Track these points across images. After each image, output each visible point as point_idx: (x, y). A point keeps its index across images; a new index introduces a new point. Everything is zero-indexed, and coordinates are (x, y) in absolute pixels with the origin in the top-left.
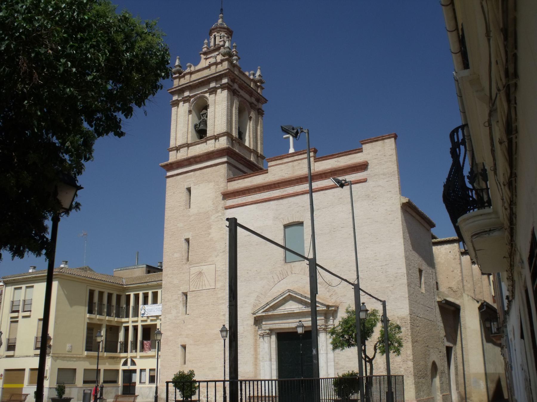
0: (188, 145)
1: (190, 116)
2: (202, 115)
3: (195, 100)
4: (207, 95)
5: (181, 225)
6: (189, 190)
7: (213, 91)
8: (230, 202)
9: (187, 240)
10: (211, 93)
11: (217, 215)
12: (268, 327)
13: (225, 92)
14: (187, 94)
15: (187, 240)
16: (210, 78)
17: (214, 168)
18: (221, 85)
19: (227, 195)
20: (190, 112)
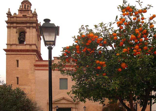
0: (16, 45)
1: (17, 34)
2: (21, 35)
3: (19, 28)
4: (25, 28)
5: (14, 72)
6: (18, 61)
7: (29, 27)
8: (36, 68)
9: (18, 78)
10: (27, 28)
11: (31, 71)
12: (54, 106)
13: (35, 30)
14: (15, 25)
15: (18, 78)
16: (27, 22)
17: (30, 55)
18: (33, 26)
19: (36, 66)
20: (17, 32)
